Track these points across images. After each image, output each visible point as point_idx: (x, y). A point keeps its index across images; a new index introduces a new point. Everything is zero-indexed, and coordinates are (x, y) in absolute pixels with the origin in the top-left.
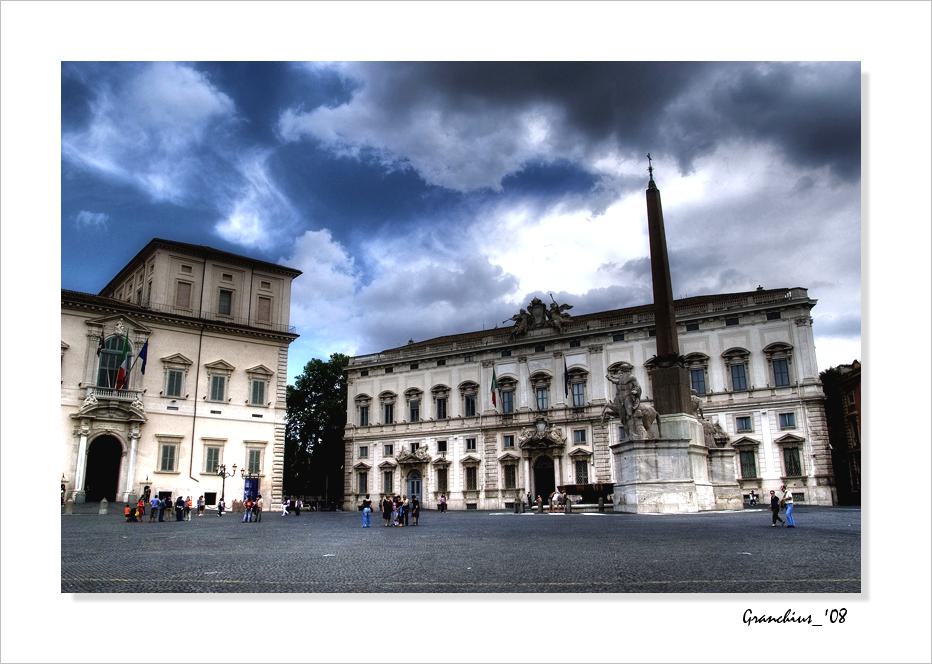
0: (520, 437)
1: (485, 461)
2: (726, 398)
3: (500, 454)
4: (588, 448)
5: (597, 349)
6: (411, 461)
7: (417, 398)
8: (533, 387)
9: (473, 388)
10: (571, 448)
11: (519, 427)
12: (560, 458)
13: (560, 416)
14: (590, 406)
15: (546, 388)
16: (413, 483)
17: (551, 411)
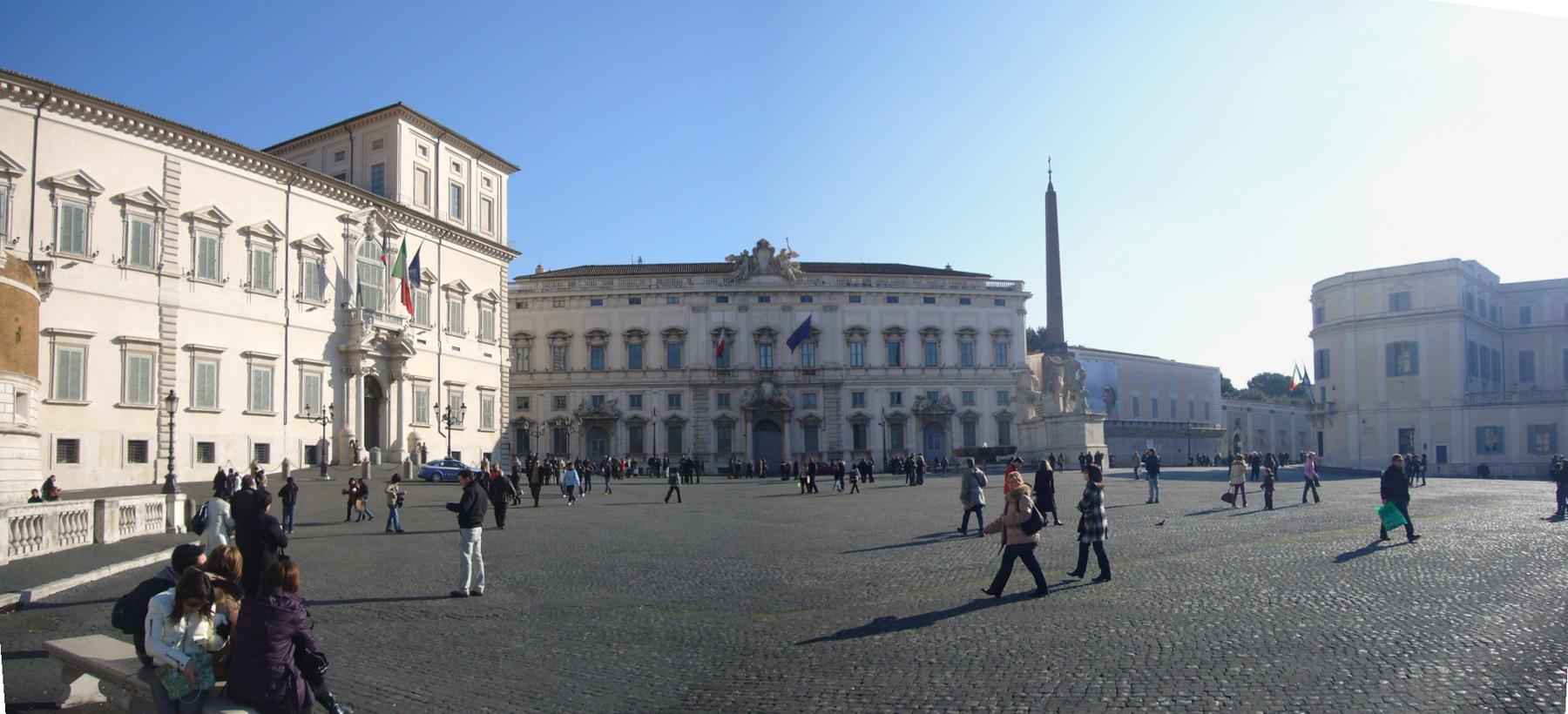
0: (738, 397)
1: (692, 419)
2: (955, 372)
3: (715, 413)
4: (819, 413)
5: (832, 309)
6: (596, 417)
7: (601, 342)
8: (756, 343)
9: (679, 336)
10: (800, 413)
11: (738, 385)
12: (789, 421)
13: (788, 377)
14: (823, 369)
15: (772, 344)
16: (595, 443)
17: (777, 371)
